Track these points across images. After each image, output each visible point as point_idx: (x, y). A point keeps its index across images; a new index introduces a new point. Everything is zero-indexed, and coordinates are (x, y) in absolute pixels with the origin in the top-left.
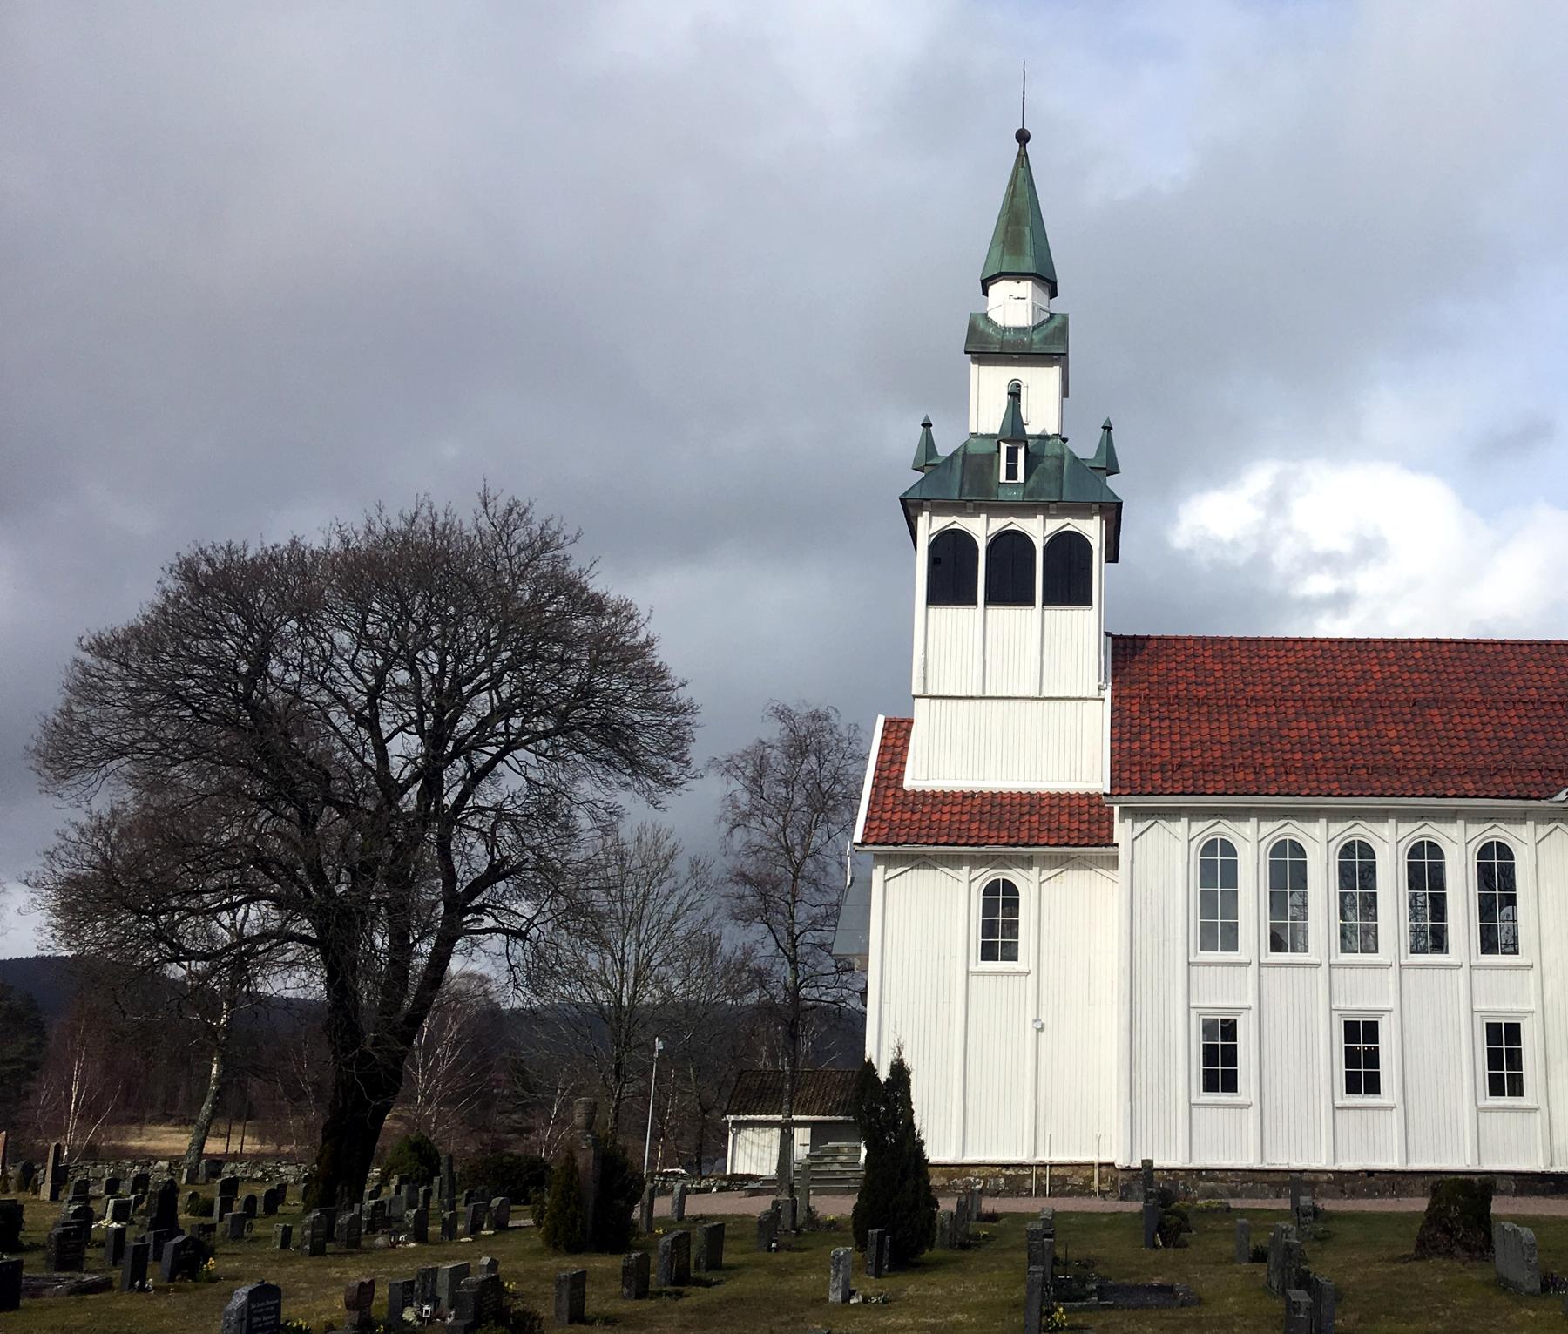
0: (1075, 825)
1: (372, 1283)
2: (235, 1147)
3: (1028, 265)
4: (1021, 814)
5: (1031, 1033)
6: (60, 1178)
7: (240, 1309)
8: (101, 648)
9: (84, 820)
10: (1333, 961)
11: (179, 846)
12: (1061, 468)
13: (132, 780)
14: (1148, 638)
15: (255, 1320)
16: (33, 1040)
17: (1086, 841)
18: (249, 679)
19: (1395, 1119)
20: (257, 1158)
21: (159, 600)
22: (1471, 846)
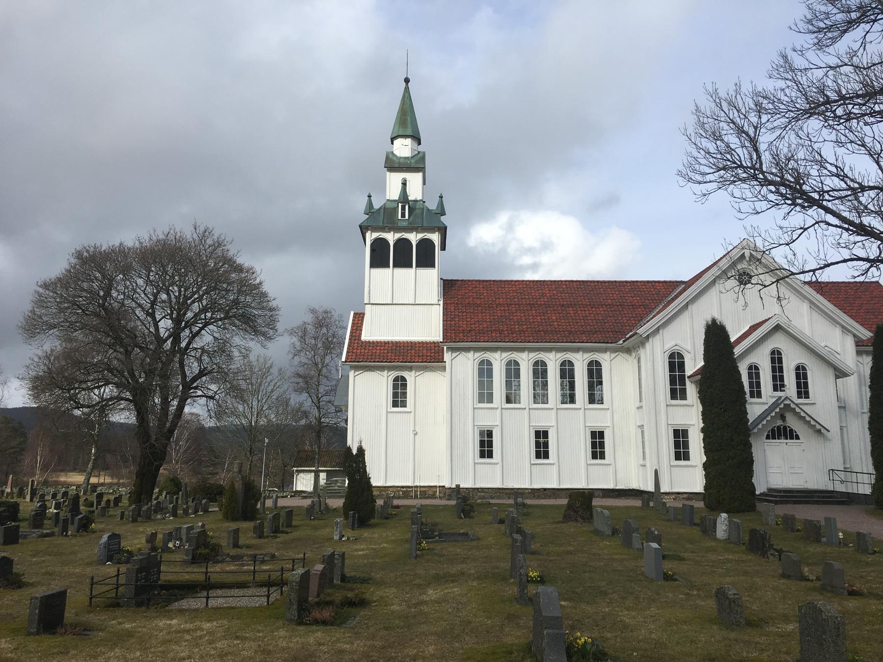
0: (429, 354)
1: (156, 532)
2: (102, 481)
4: (408, 350)
5: (412, 435)
6: (33, 493)
7: (105, 543)
8: (46, 286)
9: (40, 353)
10: (530, 407)
11: (77, 363)
13: (59, 338)
14: (458, 280)
15: (111, 547)
16: (22, 439)
17: (433, 360)
18: (104, 298)
19: (555, 468)
20: (110, 485)
21: (68, 267)
22: (585, 361)
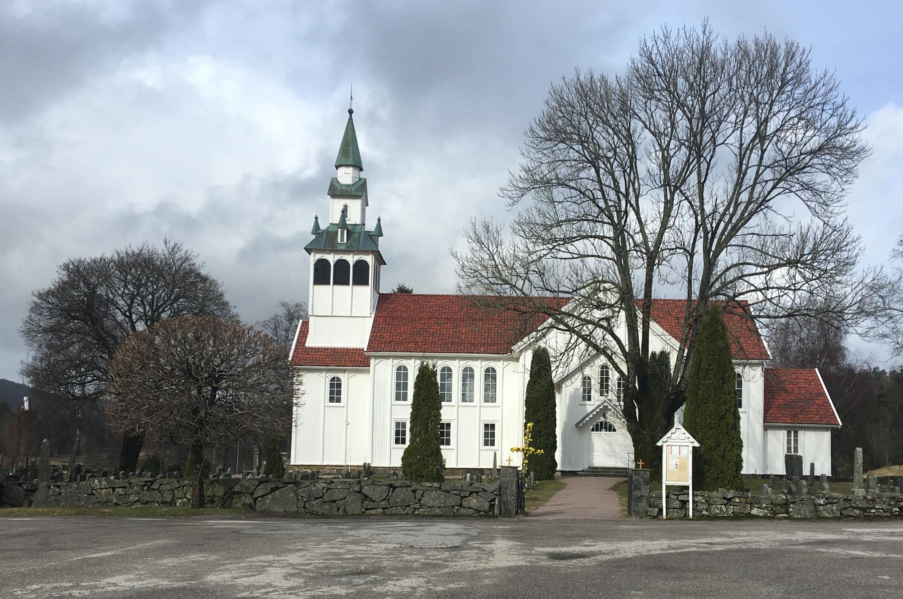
0: (360, 359)
3: (351, 162)
12: (360, 237)
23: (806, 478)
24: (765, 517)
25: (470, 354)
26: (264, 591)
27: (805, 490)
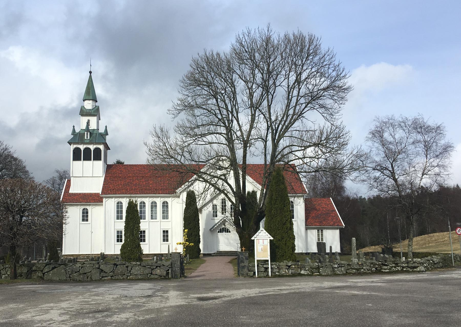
4: (89, 197)
23: (328, 254)
24: (308, 275)
25: (154, 195)
26: (48, 323)
27: (327, 260)
